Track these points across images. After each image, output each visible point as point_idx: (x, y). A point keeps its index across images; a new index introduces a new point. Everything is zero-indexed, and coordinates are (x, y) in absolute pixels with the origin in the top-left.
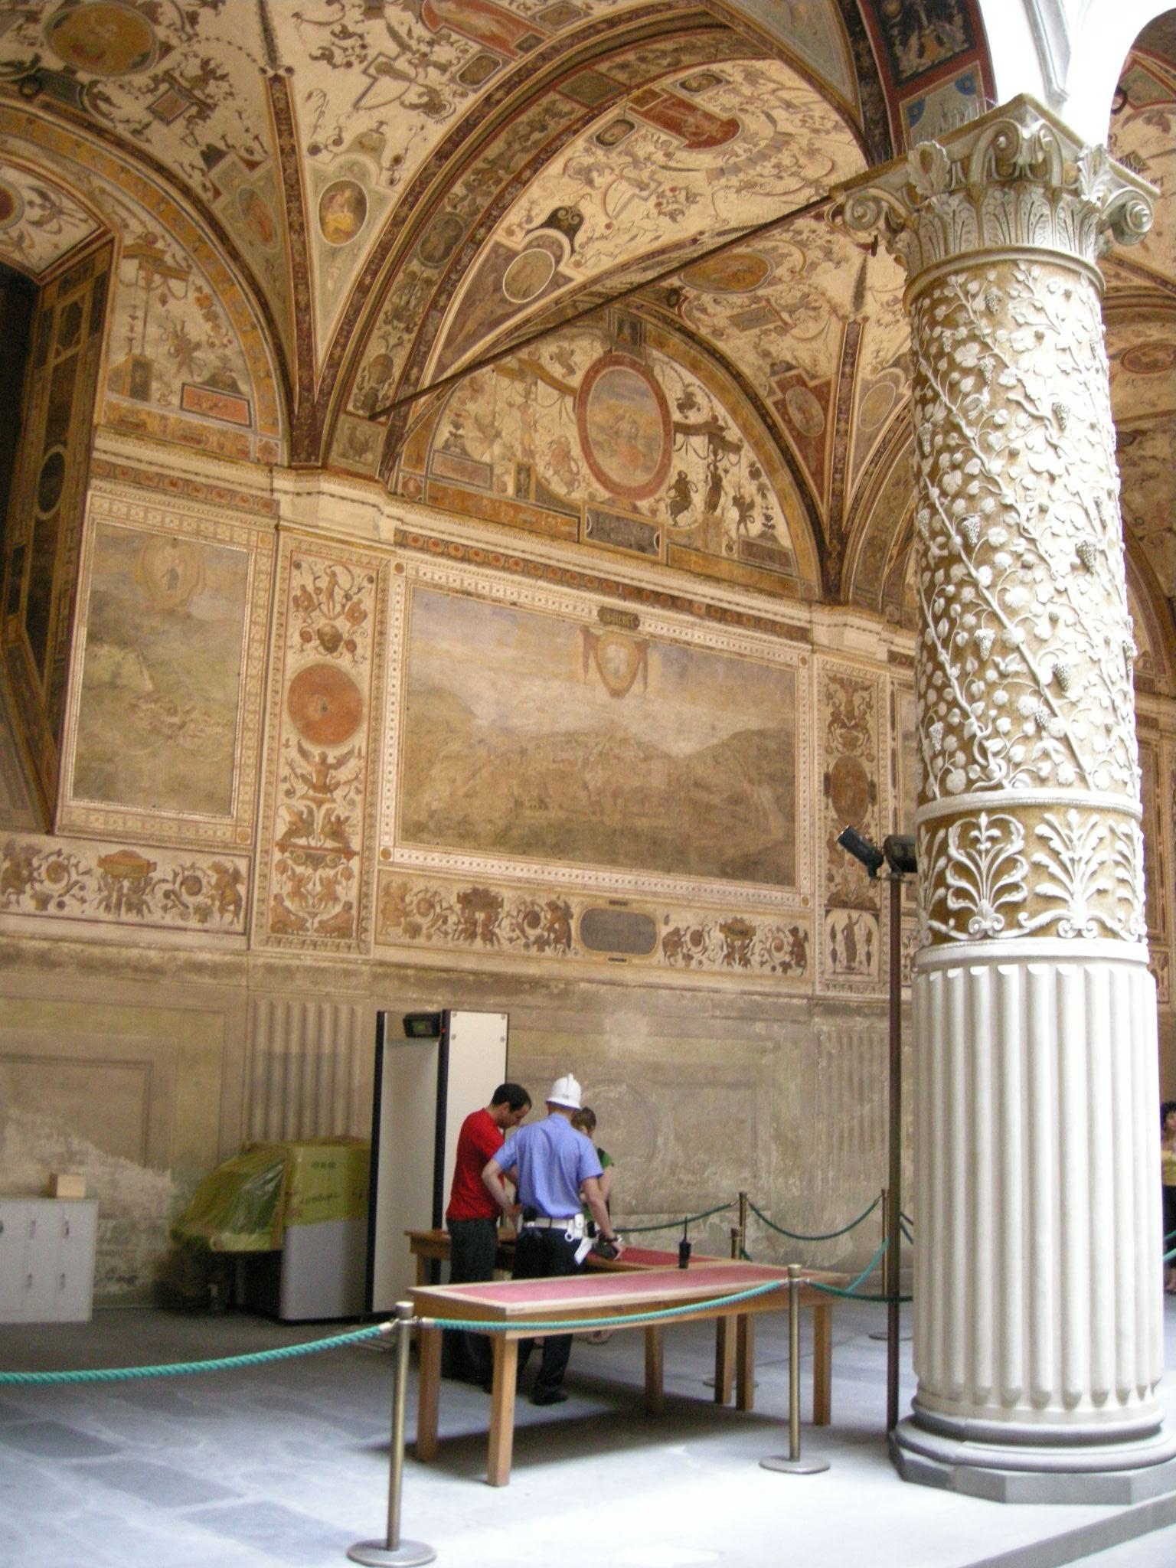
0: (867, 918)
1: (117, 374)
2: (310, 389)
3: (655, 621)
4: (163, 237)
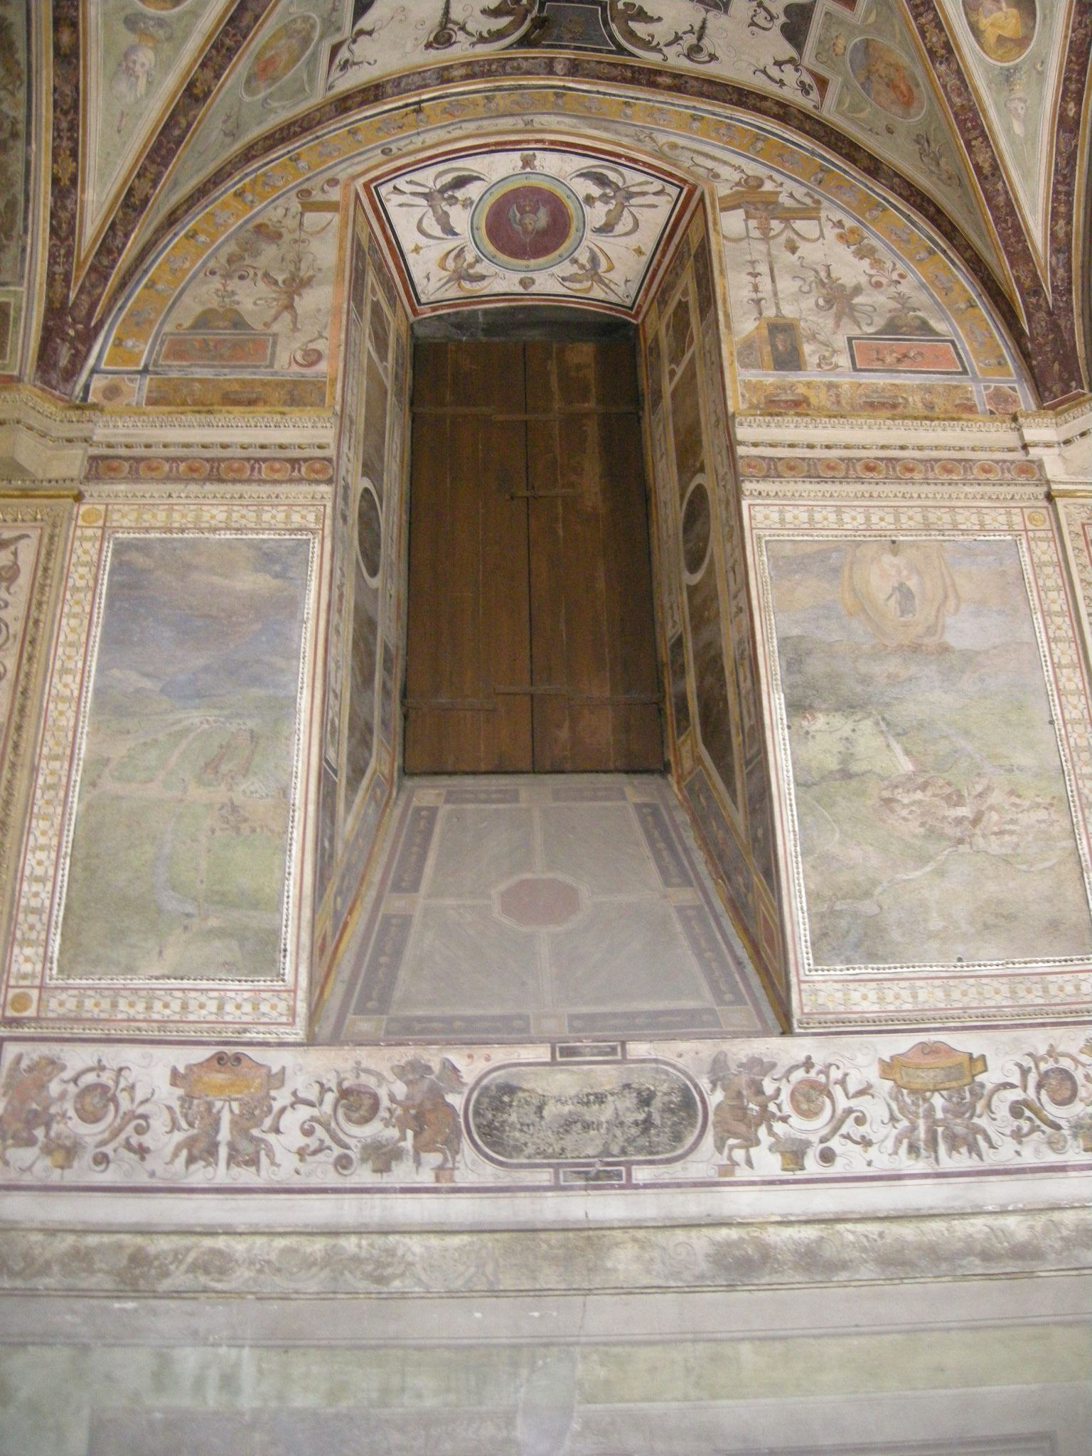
2: (1037, 291)
4: (770, 178)
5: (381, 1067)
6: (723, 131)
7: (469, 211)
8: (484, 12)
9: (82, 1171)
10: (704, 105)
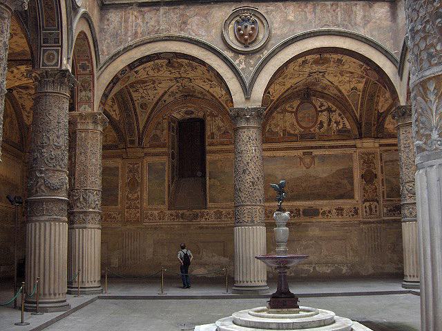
0: (376, 203)
3: (316, 152)
5: (173, 212)
9: (151, 221)
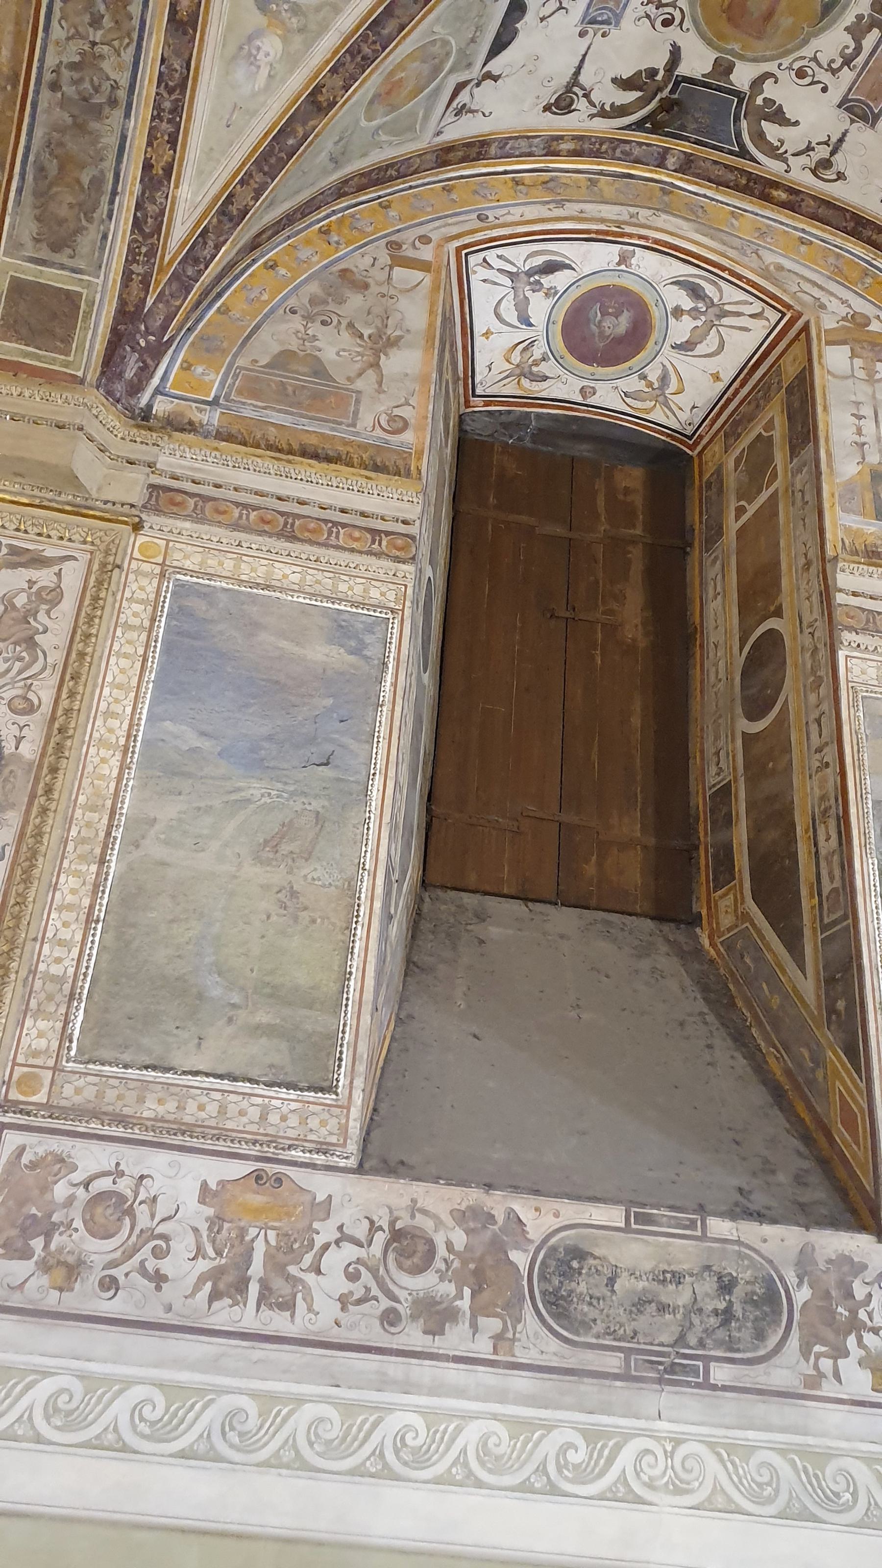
1: (850, 487)
6: (831, 260)
7: (551, 301)
8: (614, 81)
10: (815, 230)
